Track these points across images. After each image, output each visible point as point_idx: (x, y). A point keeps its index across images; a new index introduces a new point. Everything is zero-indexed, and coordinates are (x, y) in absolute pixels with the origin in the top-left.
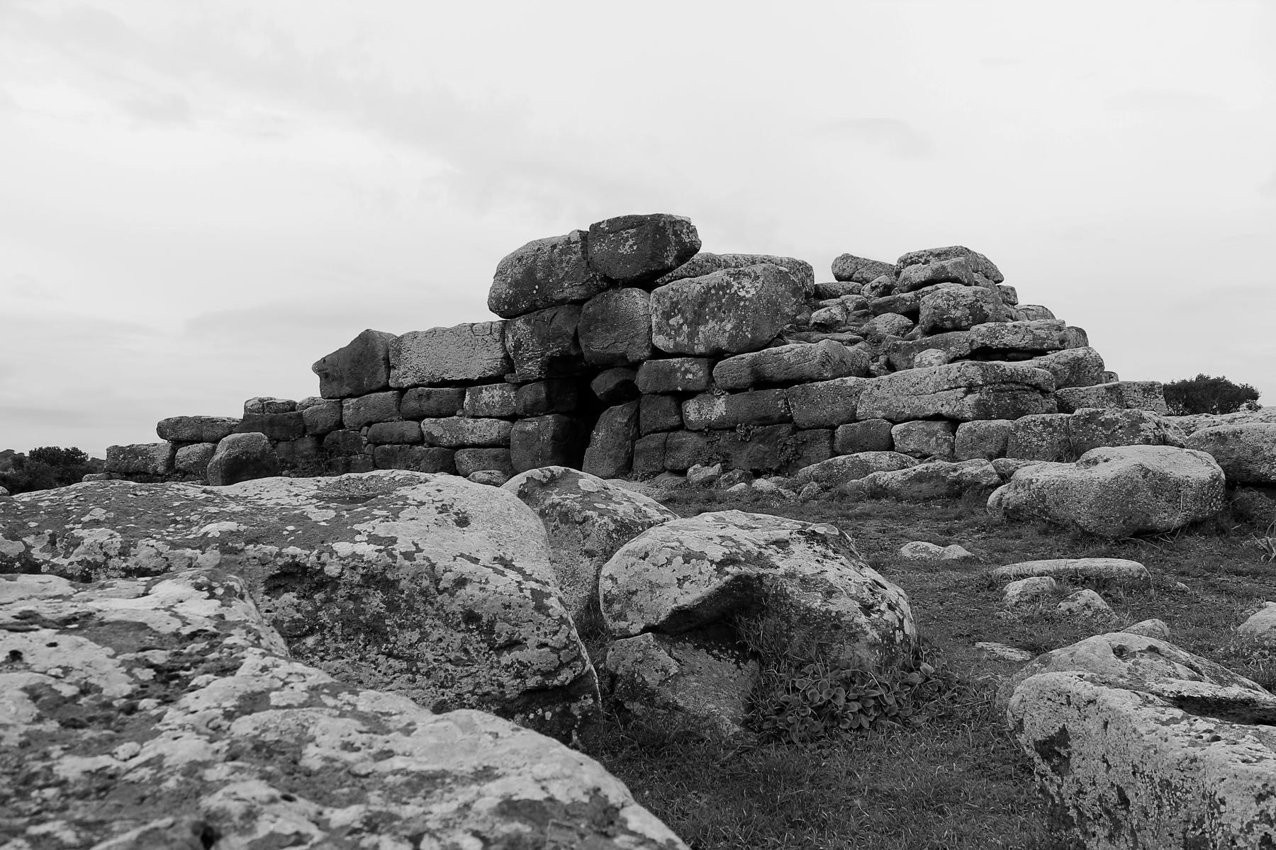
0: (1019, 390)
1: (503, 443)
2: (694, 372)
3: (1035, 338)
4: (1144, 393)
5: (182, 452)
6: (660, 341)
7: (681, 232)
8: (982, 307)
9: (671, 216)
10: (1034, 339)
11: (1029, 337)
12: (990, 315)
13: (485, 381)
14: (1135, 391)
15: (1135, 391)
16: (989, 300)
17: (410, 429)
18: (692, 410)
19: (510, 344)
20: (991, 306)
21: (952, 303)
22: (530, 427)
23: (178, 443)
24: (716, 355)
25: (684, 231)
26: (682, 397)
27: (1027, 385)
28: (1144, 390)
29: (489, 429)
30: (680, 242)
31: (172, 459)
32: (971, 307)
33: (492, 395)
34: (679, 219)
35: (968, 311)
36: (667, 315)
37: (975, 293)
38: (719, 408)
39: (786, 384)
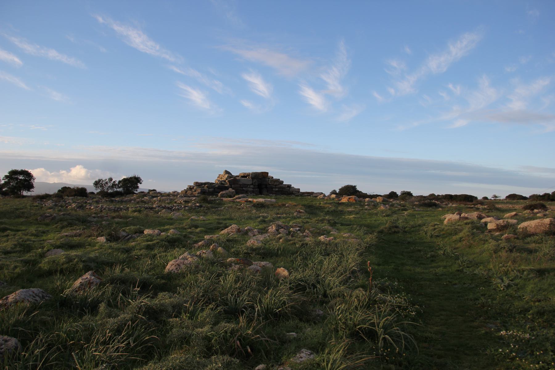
1: (253, 191)
2: (274, 186)
5: (210, 190)
6: (270, 183)
13: (250, 185)
17: (242, 189)
18: (274, 189)
19: (254, 181)
22: (256, 189)
23: (209, 188)
24: (276, 185)
26: (272, 188)
29: (251, 189)
31: (209, 191)
33: (252, 186)
36: (271, 181)
38: (277, 189)
39: (283, 188)
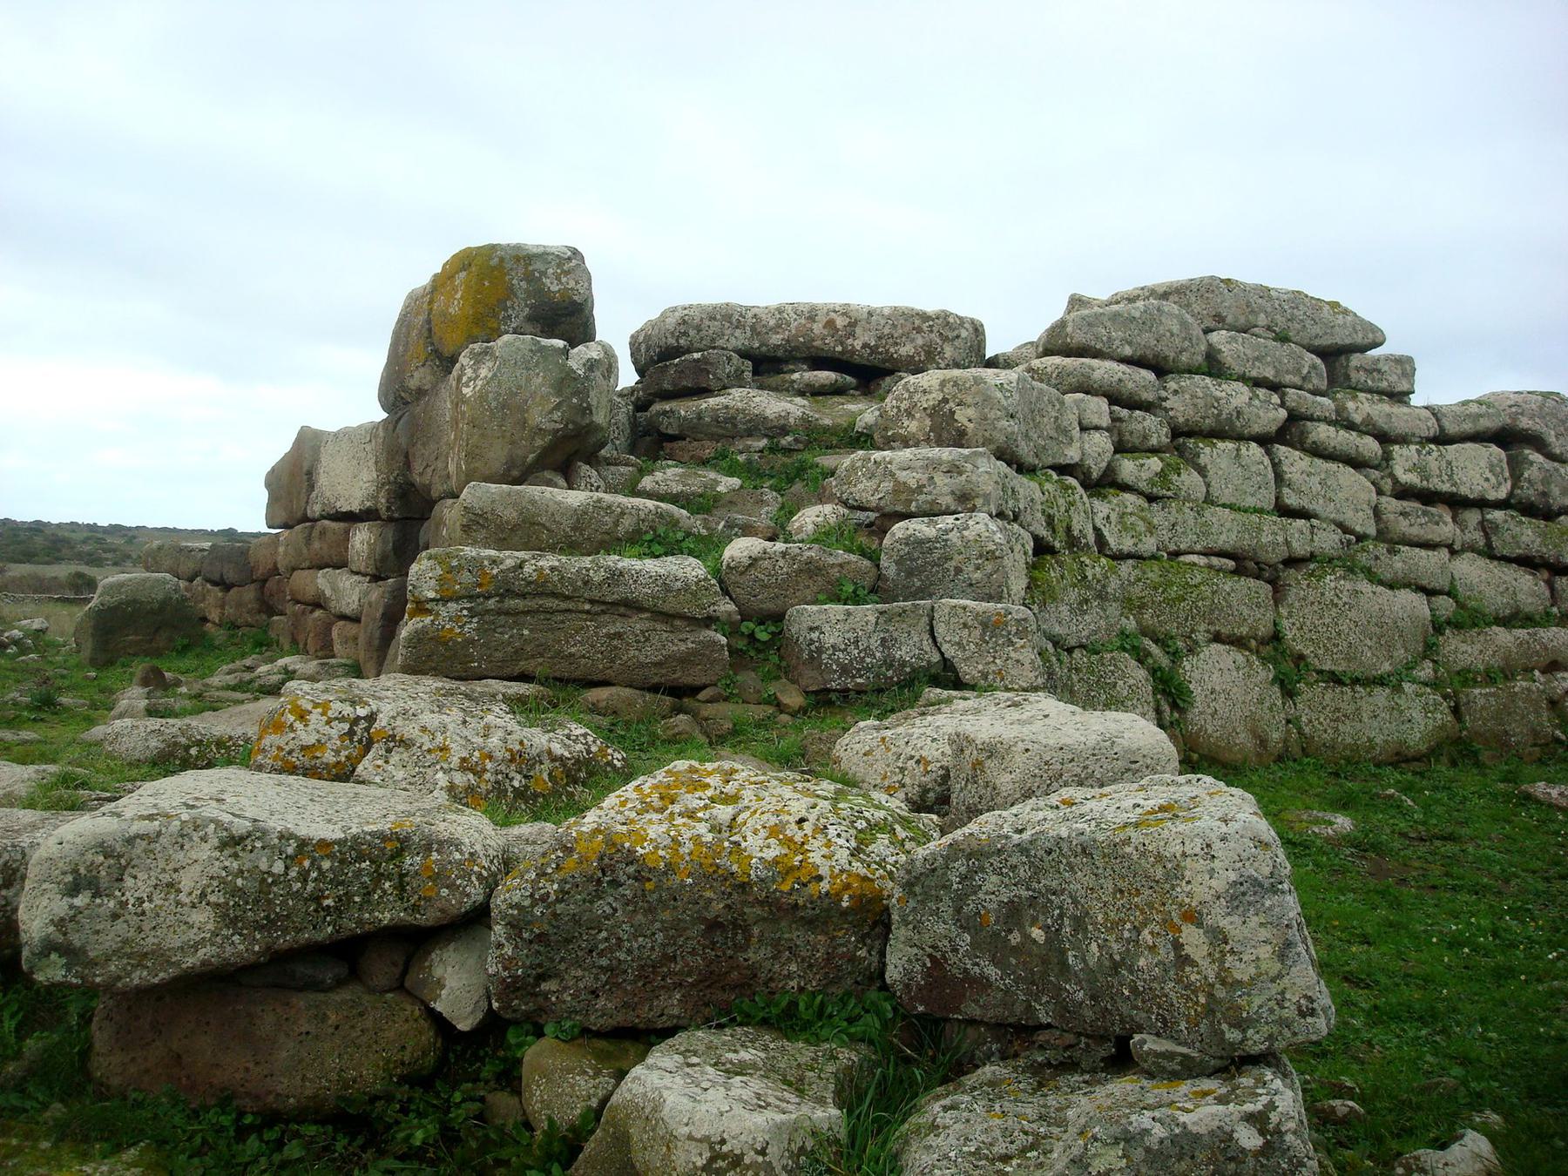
0: (568, 611)
3: (900, 489)
4: (984, 633)
7: (543, 273)
8: (952, 413)
9: (518, 247)
10: (895, 491)
11: (887, 485)
12: (969, 431)
14: (965, 625)
15: (965, 625)
16: (969, 400)
20: (971, 412)
21: (903, 406)
25: (550, 271)
27: (592, 602)
28: (985, 625)
30: (539, 292)
32: (934, 412)
34: (541, 250)
35: (928, 422)
37: (943, 384)
